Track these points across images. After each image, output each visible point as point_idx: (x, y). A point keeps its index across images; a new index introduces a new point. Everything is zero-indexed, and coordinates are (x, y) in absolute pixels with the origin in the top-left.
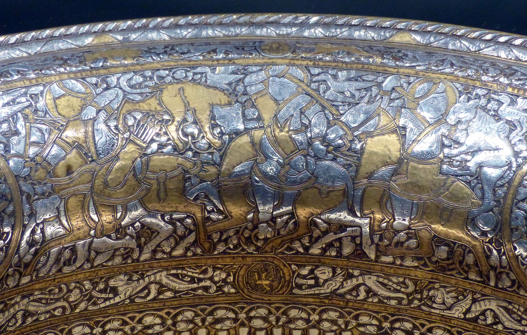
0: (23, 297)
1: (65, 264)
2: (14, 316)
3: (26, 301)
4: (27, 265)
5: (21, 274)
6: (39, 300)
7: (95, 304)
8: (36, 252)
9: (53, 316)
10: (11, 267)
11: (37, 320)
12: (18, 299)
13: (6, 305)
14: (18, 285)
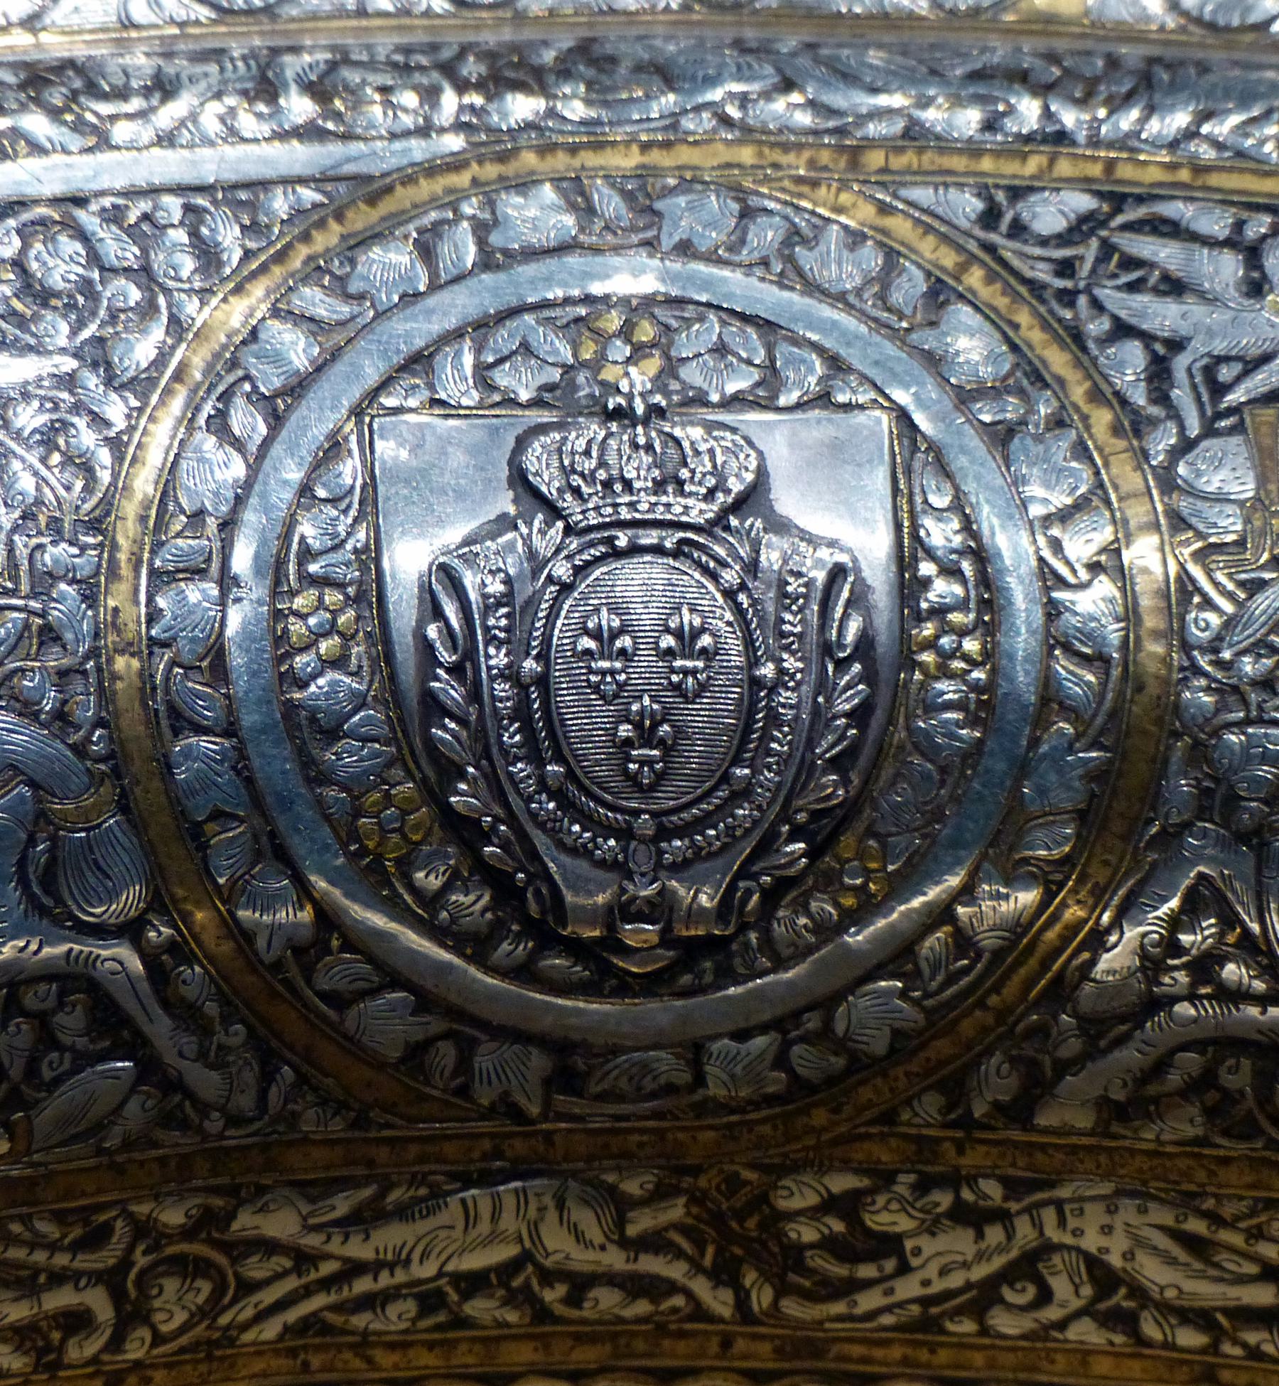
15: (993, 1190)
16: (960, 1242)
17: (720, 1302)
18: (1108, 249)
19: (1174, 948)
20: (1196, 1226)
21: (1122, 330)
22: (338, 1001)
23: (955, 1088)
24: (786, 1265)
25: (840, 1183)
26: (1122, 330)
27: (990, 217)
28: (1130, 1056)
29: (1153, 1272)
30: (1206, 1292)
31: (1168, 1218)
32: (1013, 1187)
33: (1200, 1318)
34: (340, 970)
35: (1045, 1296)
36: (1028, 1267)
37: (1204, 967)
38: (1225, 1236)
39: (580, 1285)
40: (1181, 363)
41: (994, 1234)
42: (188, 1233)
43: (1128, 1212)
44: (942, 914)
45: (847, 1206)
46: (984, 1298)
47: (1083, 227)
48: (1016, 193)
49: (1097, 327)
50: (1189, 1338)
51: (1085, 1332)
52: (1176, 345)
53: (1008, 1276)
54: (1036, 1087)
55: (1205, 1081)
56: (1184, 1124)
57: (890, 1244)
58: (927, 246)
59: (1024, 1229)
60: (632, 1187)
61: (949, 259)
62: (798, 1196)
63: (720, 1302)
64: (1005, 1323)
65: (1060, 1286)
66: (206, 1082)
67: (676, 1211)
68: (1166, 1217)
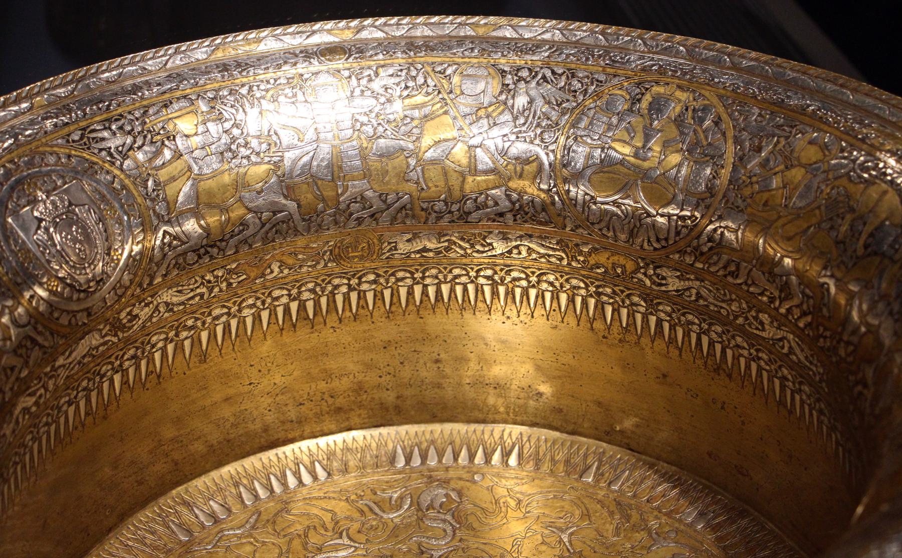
0: (697, 279)
1: (729, 274)
2: (689, 289)
3: (698, 283)
4: (702, 254)
5: (696, 258)
6: (710, 291)
7: (750, 325)
8: (711, 249)
9: (719, 312)
10: (689, 246)
11: (707, 306)
12: (692, 277)
13: (682, 275)
14: (692, 265)
15: (149, 299)
16: (147, 309)
17: (115, 340)
18: (88, 138)
19: (164, 244)
20: (180, 288)
21: (101, 150)
22: (57, 319)
23: (140, 285)
24: (123, 328)
25: (128, 310)
26: (101, 150)
27: (68, 141)
28: (165, 265)
29: (175, 300)
30: (183, 298)
31: (175, 289)
32: (152, 296)
33: (183, 303)
34: (56, 315)
35: (160, 312)
36: (157, 308)
37: (170, 245)
38: (185, 287)
39: (97, 348)
40: (112, 150)
41: (151, 306)
42: (51, 371)
43: (170, 291)
44: (130, 256)
45: (129, 314)
46: (151, 316)
47: (81, 138)
48: (69, 135)
49: (96, 151)
50: (181, 307)
51: (167, 315)
52: (110, 148)
53: (154, 312)
54: (152, 278)
55: (177, 263)
56: (175, 272)
57: (137, 316)
58: (62, 150)
59: (155, 303)
60: (101, 327)
61: (67, 151)
62: (123, 315)
63: (115, 340)
64: (154, 320)
65: (162, 309)
66: (46, 344)
67: (108, 327)
68: (175, 289)
